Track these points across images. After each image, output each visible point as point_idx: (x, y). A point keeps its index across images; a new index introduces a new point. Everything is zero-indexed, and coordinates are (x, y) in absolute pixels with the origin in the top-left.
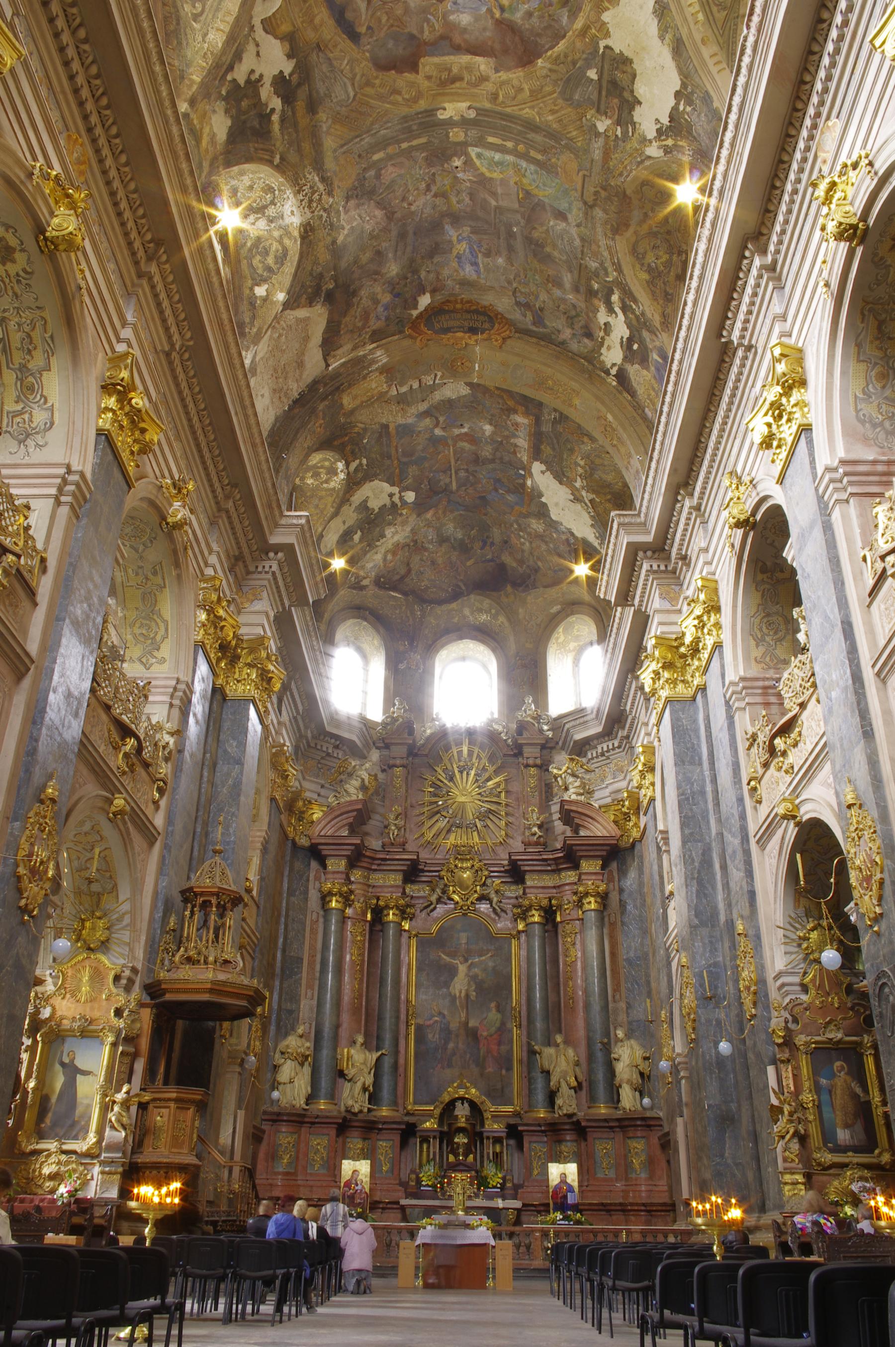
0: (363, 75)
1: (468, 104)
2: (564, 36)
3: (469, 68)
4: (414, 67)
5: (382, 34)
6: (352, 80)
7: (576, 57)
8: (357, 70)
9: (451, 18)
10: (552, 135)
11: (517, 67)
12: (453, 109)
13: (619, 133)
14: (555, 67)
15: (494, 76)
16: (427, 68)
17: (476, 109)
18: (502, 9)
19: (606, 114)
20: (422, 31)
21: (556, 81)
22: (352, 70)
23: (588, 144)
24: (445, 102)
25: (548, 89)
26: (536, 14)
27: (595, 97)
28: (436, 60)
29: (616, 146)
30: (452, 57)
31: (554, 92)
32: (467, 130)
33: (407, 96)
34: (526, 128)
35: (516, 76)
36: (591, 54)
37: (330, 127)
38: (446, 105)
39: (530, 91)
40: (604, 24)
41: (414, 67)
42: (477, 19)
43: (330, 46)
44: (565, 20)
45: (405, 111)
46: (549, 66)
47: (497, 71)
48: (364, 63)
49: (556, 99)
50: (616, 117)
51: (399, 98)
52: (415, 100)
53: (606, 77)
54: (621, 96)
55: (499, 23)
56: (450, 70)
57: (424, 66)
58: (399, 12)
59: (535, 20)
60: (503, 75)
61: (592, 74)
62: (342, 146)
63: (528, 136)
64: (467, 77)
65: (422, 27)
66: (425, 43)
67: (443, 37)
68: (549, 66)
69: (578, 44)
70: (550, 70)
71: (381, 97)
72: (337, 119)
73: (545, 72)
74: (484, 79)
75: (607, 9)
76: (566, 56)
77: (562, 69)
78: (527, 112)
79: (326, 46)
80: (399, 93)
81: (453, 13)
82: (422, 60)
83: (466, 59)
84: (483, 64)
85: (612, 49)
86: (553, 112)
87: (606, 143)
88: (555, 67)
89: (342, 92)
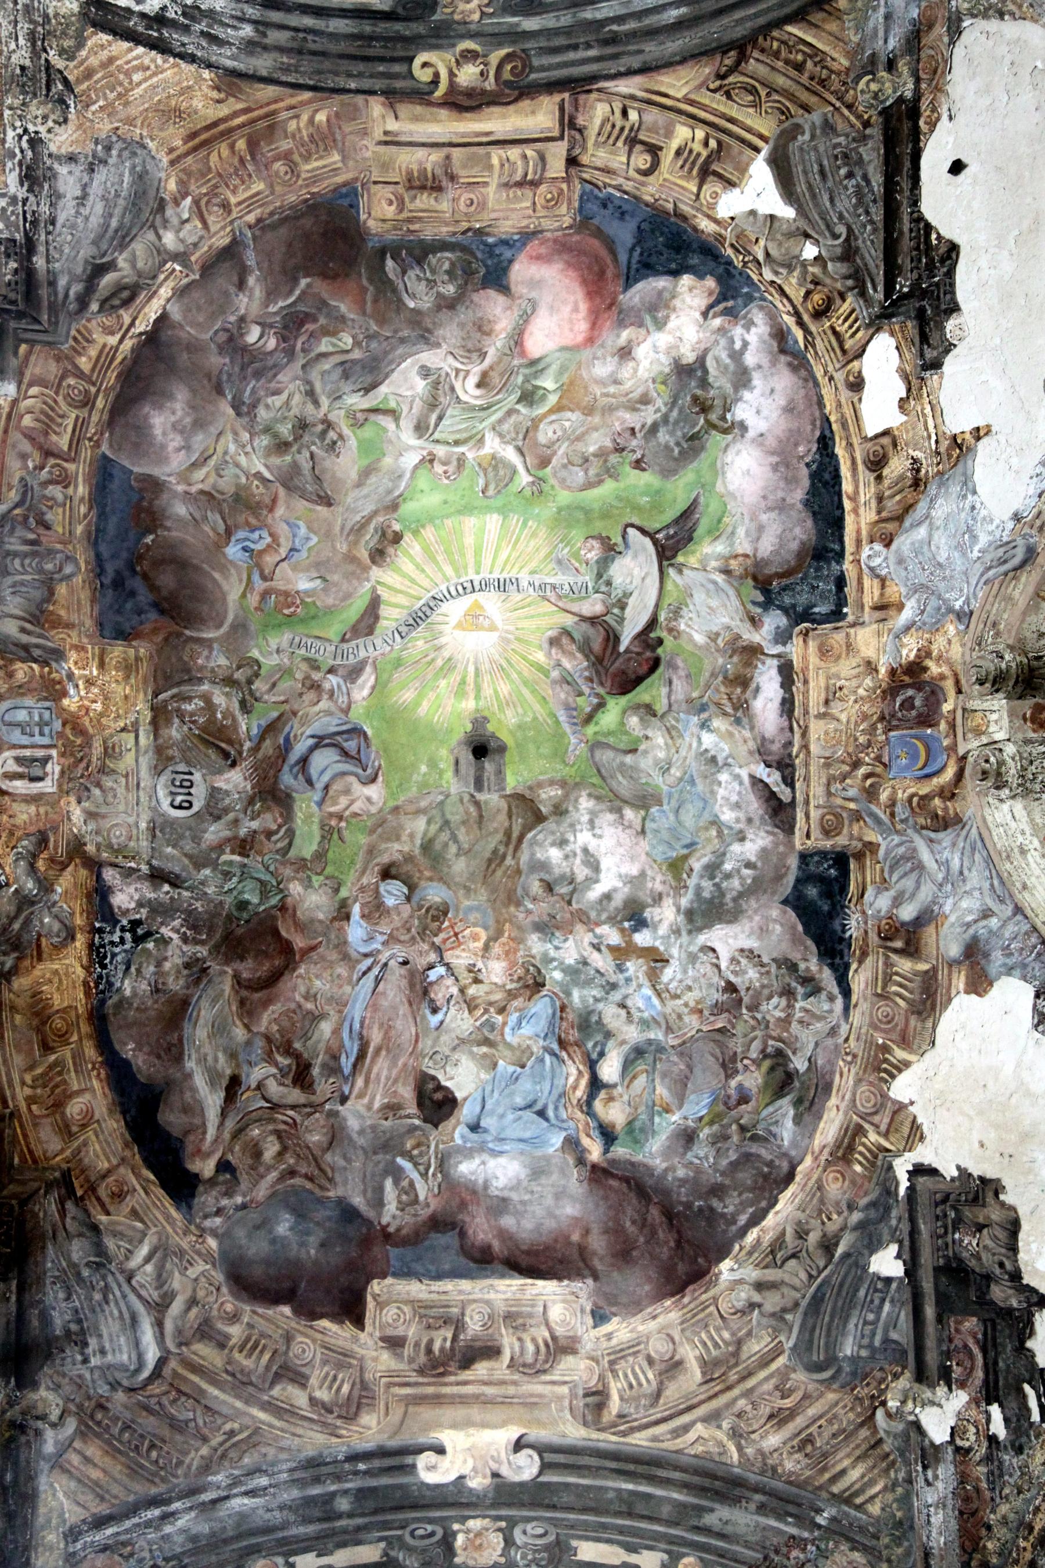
0: (193, 1302)
1: (513, 1433)
2: (790, 1177)
3: (514, 1318)
4: (352, 1310)
5: (262, 1191)
6: (159, 1308)
7: (832, 1227)
8: (176, 1282)
9: (466, 1168)
10: (786, 1500)
11: (659, 1296)
12: (467, 1450)
13: (998, 1427)
14: (772, 1275)
15: (591, 1337)
16: (390, 1313)
17: (541, 1449)
18: (608, 1135)
19: (946, 1376)
20: (379, 1203)
21: (779, 1316)
22: (161, 1279)
23: (905, 1500)
24: (439, 1426)
25: (755, 1347)
26: (705, 1133)
27: (902, 1334)
28: (417, 1289)
29: (996, 1476)
30: (465, 1285)
31: (777, 1352)
32: (512, 1522)
33: (323, 1395)
34: (701, 1491)
35: (656, 1326)
36: (873, 1204)
37: (67, 1446)
38: (446, 1437)
39: (707, 1365)
40: (900, 1108)
41: (352, 1310)
42: (537, 1172)
43: (102, 1192)
44: (787, 1131)
45: (314, 1441)
46: (752, 1273)
47: (599, 1317)
48: (201, 1267)
49: (787, 1370)
50: (979, 1374)
51: (300, 1398)
52: (351, 1409)
53: (927, 1258)
54: (983, 1304)
55: (598, 1175)
56: (459, 1325)
57: (381, 1305)
58: (315, 1138)
59: (702, 1152)
60: (620, 1330)
61: (887, 1263)
62: (100, 1522)
63: (710, 1520)
64: (508, 1343)
65: (380, 1190)
66: (386, 1236)
67: (438, 1223)
68: (752, 1273)
69: (835, 1189)
70: (760, 1286)
71: (240, 1383)
72: (91, 1415)
73: (744, 1294)
74: (560, 1347)
75: (904, 1066)
76: (801, 1234)
77: (794, 1272)
78: (702, 1439)
79: (92, 1189)
80: (300, 1379)
81: (468, 1153)
82: (376, 1286)
83: (506, 1289)
84: (557, 1301)
85: (933, 1172)
86: (779, 1418)
87: (963, 1478)
88: (772, 1275)
89: (128, 1344)
